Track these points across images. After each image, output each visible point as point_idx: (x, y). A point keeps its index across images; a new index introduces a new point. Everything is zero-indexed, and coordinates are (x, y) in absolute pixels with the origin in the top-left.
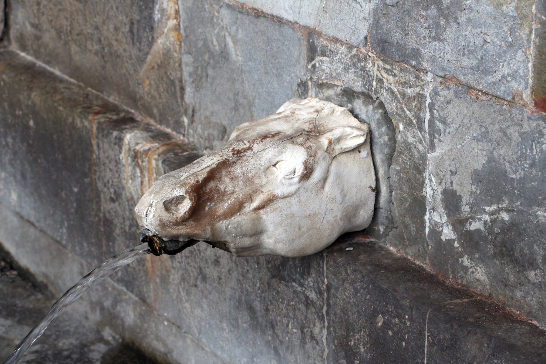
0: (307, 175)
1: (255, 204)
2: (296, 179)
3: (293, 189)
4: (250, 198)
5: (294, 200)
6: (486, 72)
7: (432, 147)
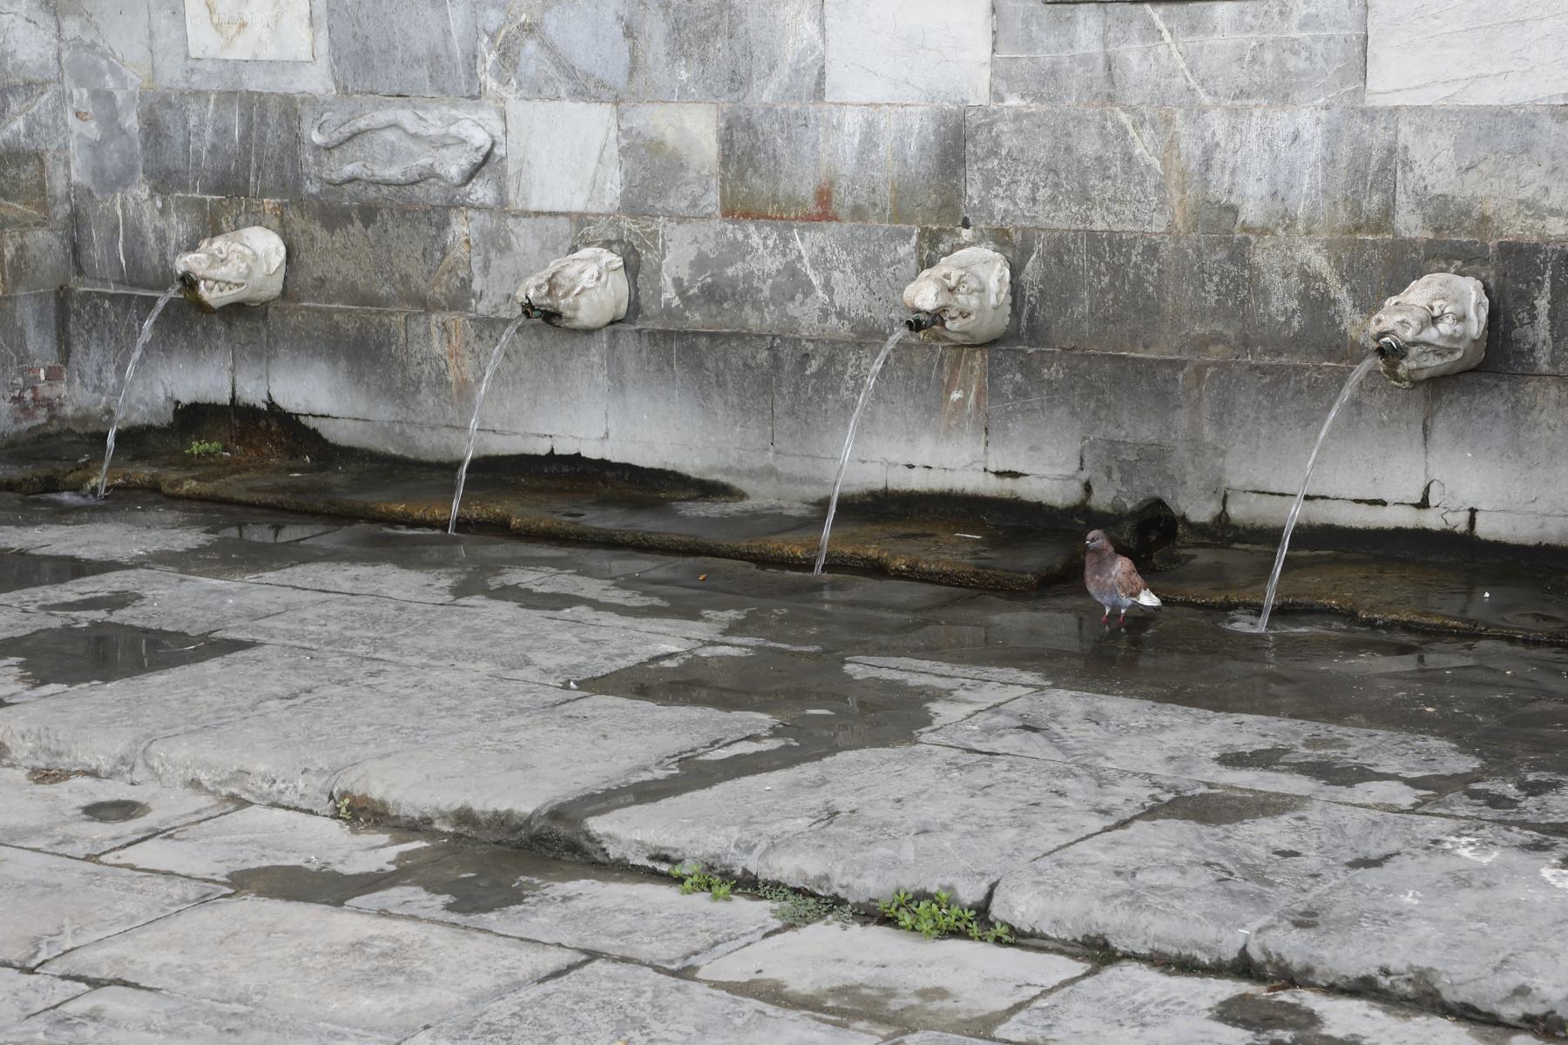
0: (598, 279)
3: (592, 285)
4: (573, 288)
6: (695, 206)
7: (663, 256)
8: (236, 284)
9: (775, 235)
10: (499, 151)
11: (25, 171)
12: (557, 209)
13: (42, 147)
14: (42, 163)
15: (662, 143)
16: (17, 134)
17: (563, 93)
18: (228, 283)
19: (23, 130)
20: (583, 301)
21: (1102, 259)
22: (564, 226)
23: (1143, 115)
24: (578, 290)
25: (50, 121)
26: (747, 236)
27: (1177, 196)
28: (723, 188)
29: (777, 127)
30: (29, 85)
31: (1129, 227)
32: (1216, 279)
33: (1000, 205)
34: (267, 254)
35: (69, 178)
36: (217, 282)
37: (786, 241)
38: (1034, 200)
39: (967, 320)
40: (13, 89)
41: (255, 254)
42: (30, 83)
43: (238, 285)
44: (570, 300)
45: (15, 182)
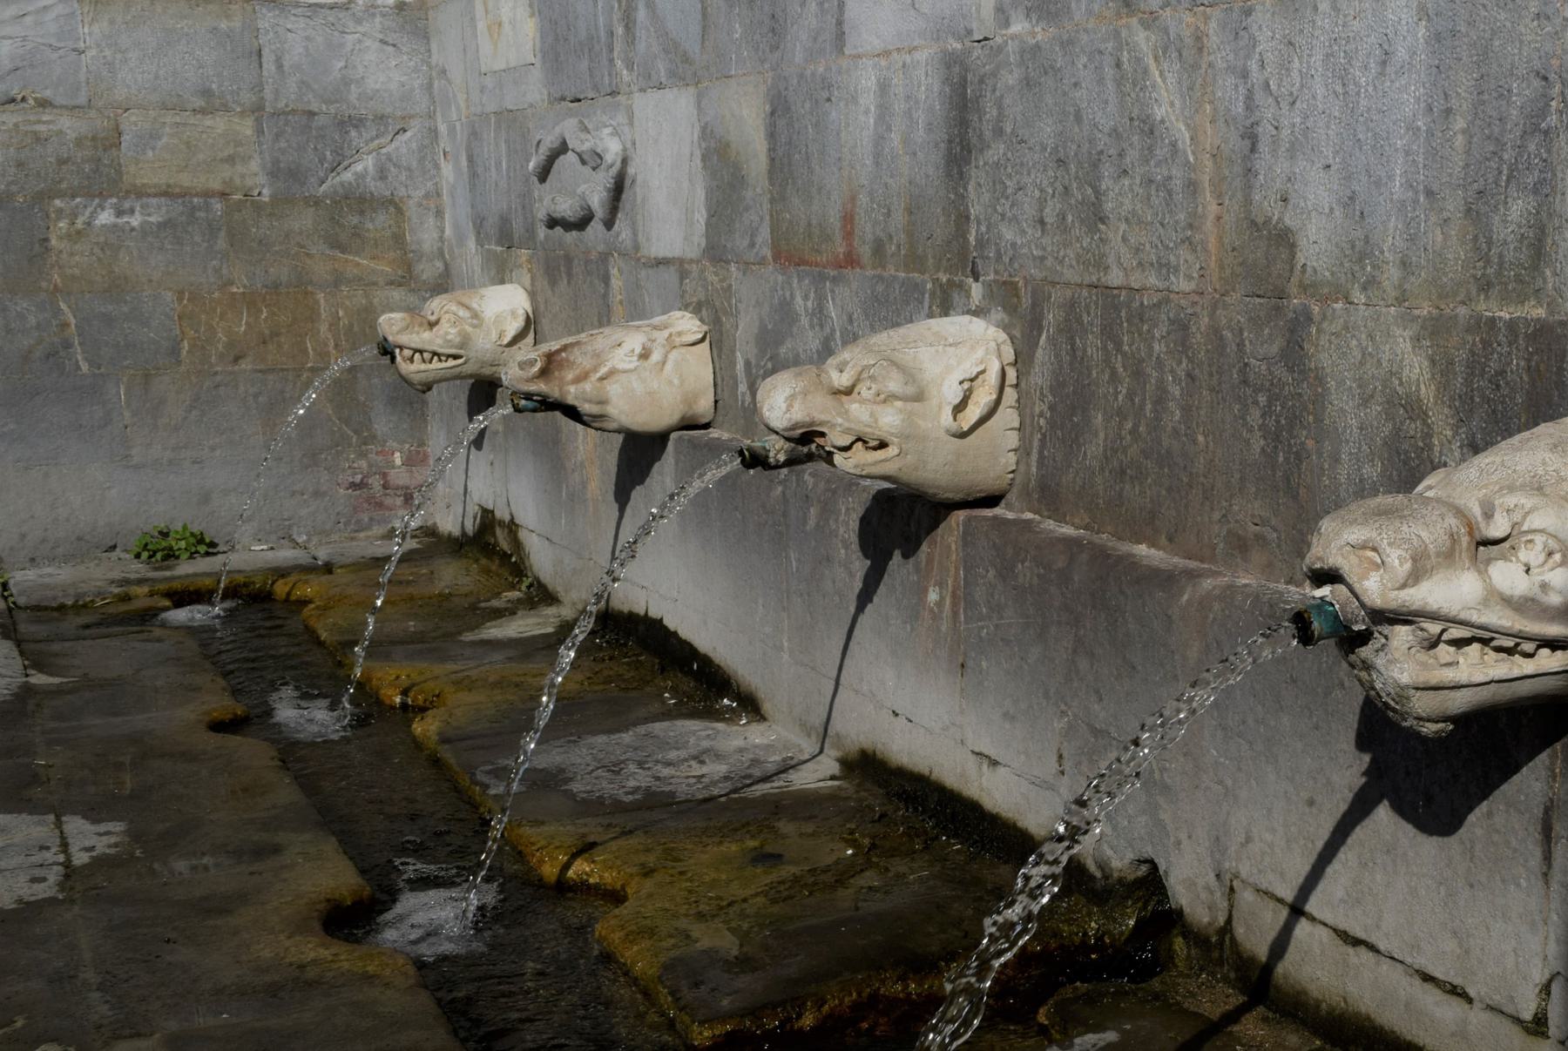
0: (645, 355)
1: (598, 375)
2: (636, 358)
3: (632, 366)
4: (595, 369)
5: (633, 377)
8: (449, 356)
9: (812, 295)
10: (631, 171)
11: (372, 220)
12: (669, 255)
13: (402, 192)
14: (400, 211)
15: (728, 145)
16: (360, 177)
17: (663, 80)
18: (435, 354)
19: (371, 168)
20: (614, 389)
21: (1118, 345)
22: (670, 276)
23: (1166, 31)
24: (603, 371)
25: (414, 164)
26: (792, 296)
27: (1213, 208)
28: (771, 216)
29: (807, 105)
30: (381, 118)
31: (1153, 280)
32: (1262, 399)
33: (1008, 234)
34: (499, 319)
35: (443, 231)
36: (421, 352)
37: (821, 299)
38: (1042, 222)
39: (880, 455)
40: (358, 122)
41: (475, 315)
42: (382, 117)
43: (455, 357)
44: (587, 386)
45: (357, 233)
